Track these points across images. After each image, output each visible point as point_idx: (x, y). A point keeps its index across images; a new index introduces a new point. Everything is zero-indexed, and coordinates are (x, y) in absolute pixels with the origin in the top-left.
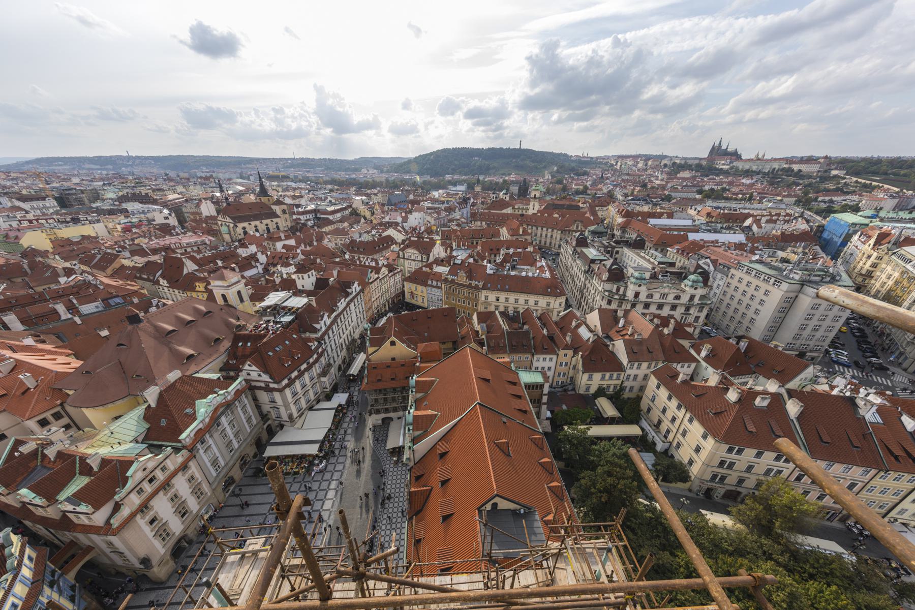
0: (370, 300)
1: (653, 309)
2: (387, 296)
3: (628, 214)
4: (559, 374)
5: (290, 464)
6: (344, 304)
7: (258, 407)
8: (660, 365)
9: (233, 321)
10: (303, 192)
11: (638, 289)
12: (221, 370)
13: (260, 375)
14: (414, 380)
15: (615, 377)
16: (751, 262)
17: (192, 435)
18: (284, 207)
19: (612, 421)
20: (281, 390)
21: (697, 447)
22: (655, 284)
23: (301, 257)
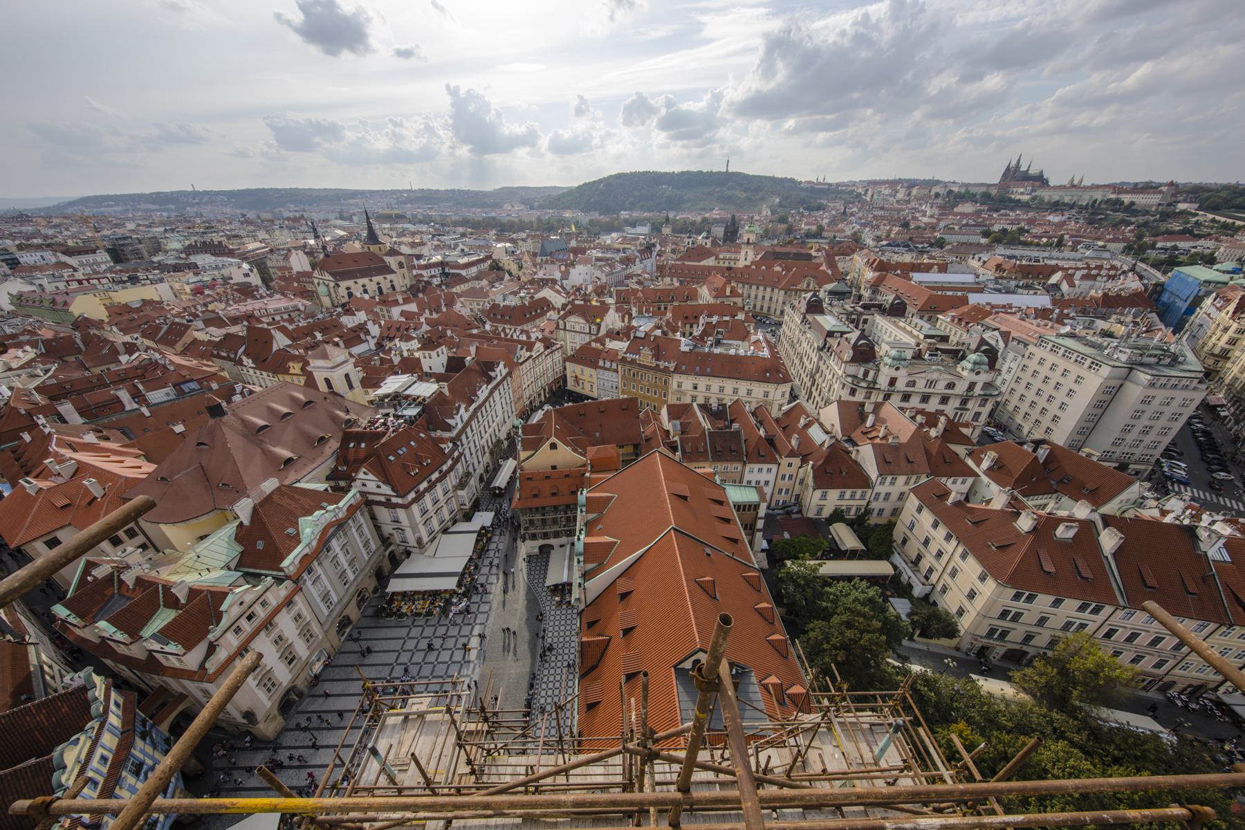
1: (915, 402)
2: (542, 382)
3: (883, 267)
4: (780, 490)
6: (486, 393)
7: (378, 528)
8: (924, 479)
9: (341, 414)
10: (425, 238)
11: (894, 374)
12: (328, 479)
13: (379, 487)
15: (858, 496)
16: (1059, 335)
17: (297, 562)
18: (401, 258)
19: (852, 555)
20: (406, 507)
21: (970, 591)
23: (425, 328)
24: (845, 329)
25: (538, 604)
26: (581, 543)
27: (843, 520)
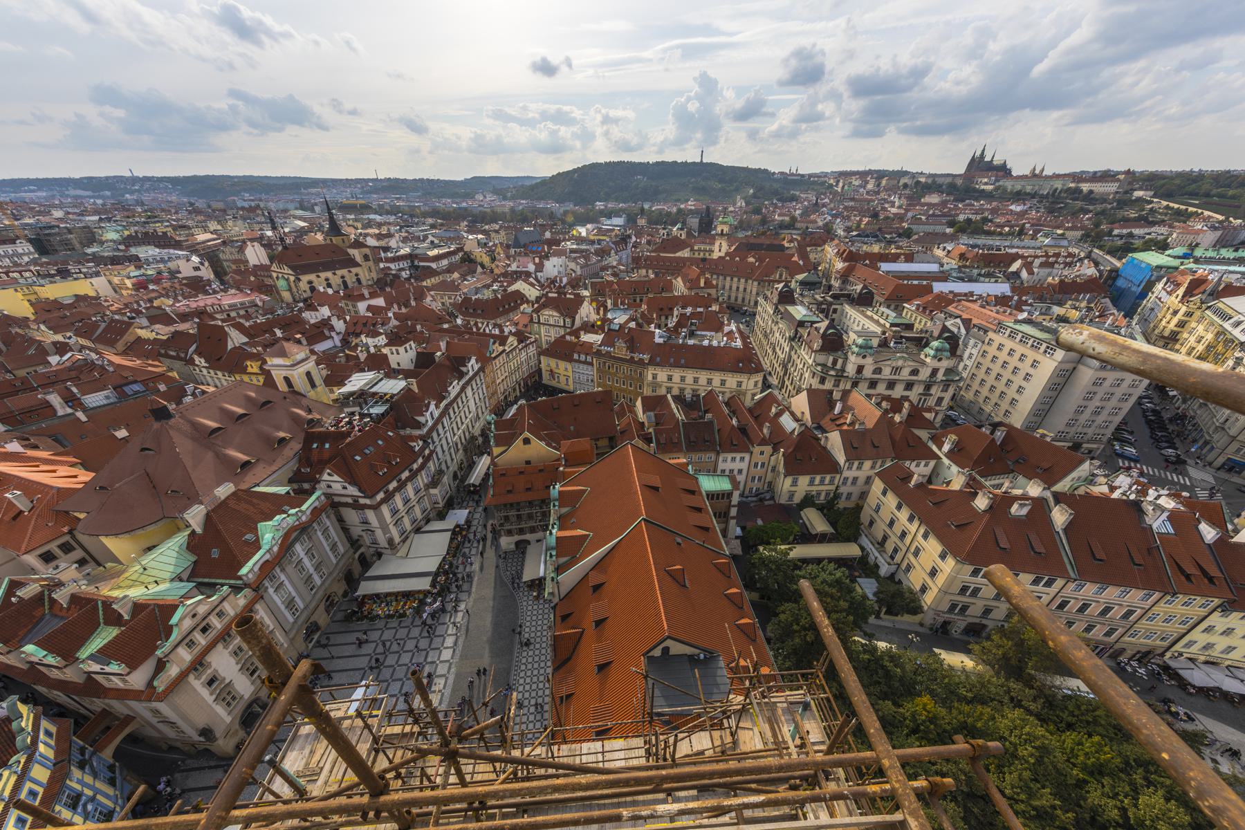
0: (494, 382)
1: (881, 389)
2: (517, 376)
3: (852, 258)
4: (753, 478)
6: (458, 389)
10: (392, 229)
11: (861, 361)
12: (290, 481)
13: (345, 488)
15: (827, 481)
17: (256, 569)
18: (367, 251)
19: (822, 538)
20: (375, 507)
21: (932, 569)
22: (886, 355)
24: (815, 319)
26: (554, 537)
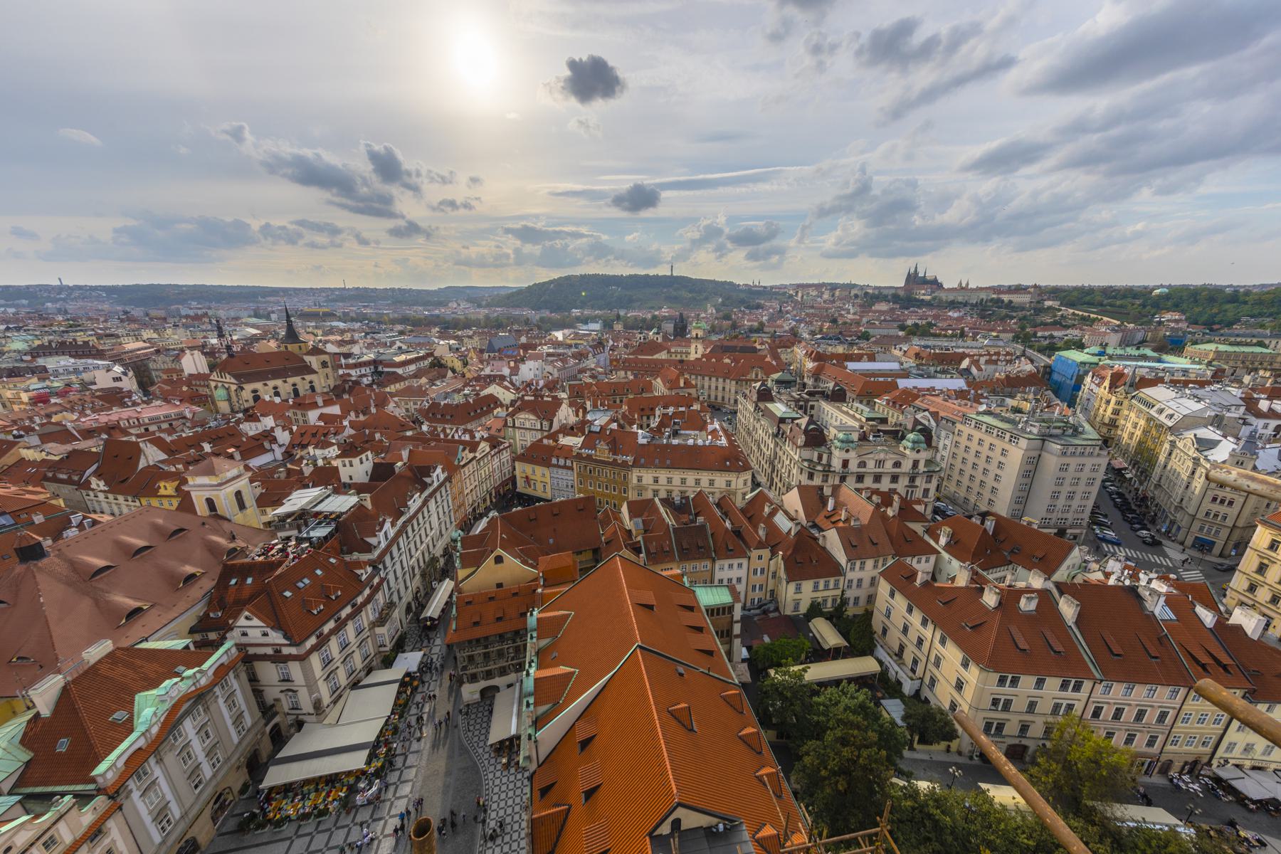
0: (461, 492)
1: (868, 482)
2: (488, 485)
3: (819, 357)
4: (754, 587)
5: (312, 796)
6: (419, 503)
7: (258, 693)
8: (890, 562)
9: (222, 541)
11: (846, 456)
14: (532, 620)
15: (831, 586)
16: (979, 413)
19: (836, 654)
20: (301, 658)
21: (958, 680)
22: (866, 449)
25: (478, 772)
27: (821, 614)
